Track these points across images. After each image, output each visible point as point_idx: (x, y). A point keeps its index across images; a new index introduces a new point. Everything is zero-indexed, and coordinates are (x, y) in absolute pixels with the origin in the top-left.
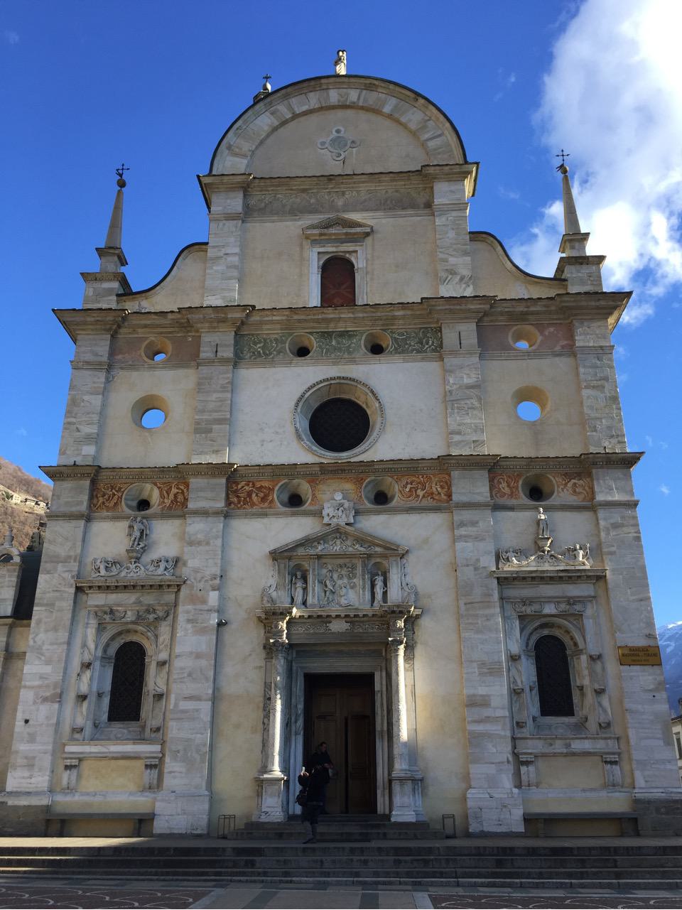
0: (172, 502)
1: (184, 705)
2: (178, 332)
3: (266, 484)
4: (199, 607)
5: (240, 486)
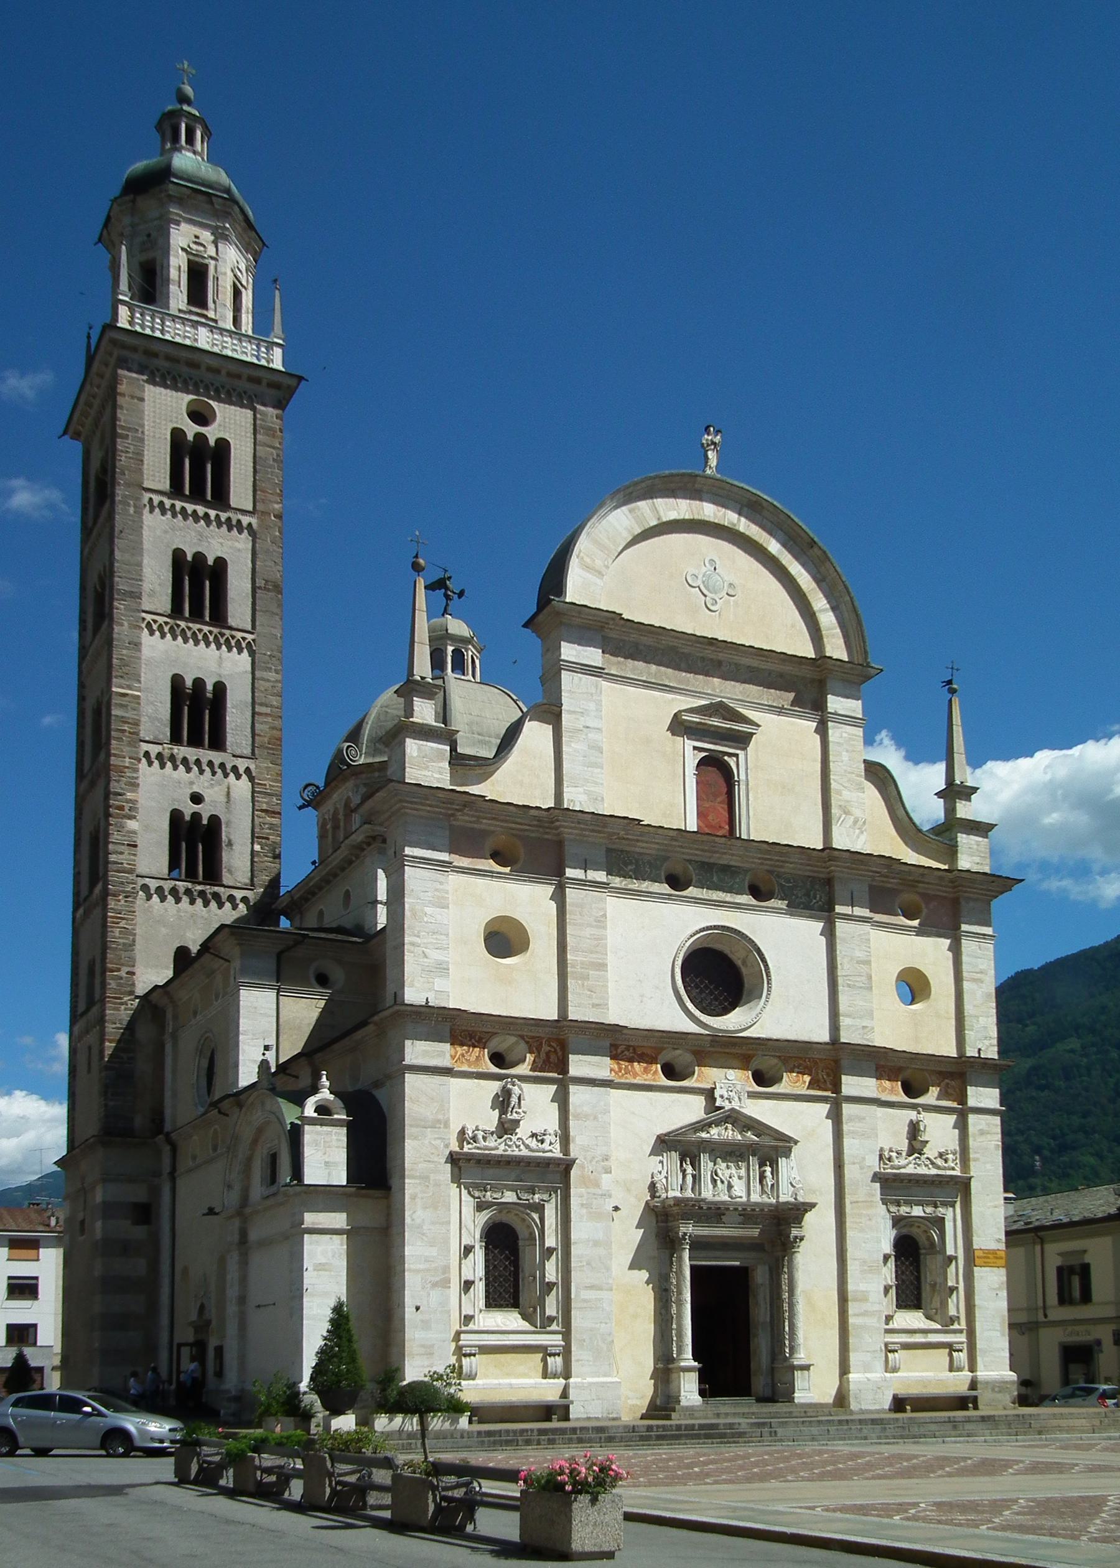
0: (544, 1061)
1: (586, 1294)
2: (533, 831)
3: (649, 1052)
4: (592, 1190)
5: (619, 1051)
